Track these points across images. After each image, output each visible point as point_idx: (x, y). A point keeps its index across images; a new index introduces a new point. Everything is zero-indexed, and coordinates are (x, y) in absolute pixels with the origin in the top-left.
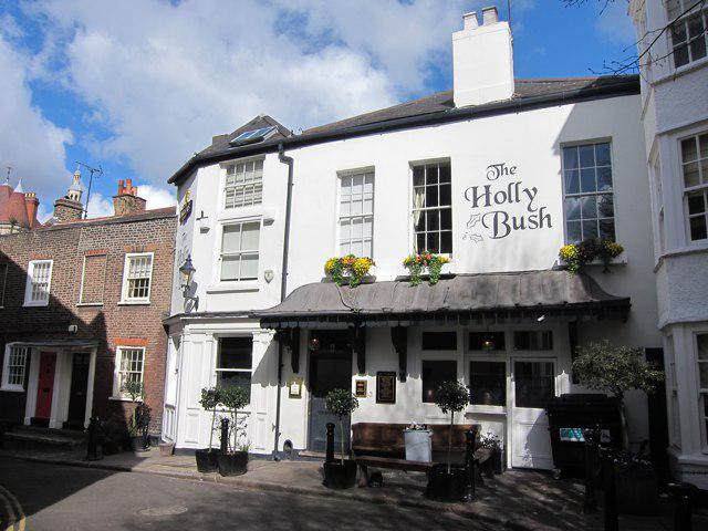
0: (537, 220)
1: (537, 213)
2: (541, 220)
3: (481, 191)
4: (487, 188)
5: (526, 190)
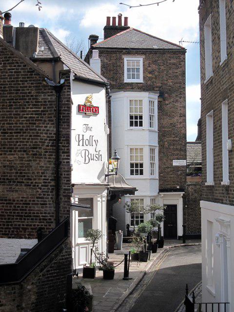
0: (97, 156)
1: (98, 153)
3: (81, 138)
4: (83, 136)
5: (95, 141)
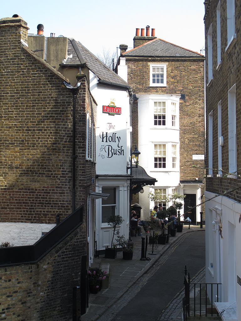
0: (120, 152)
1: (120, 148)
2: (121, 152)
5: (117, 137)
